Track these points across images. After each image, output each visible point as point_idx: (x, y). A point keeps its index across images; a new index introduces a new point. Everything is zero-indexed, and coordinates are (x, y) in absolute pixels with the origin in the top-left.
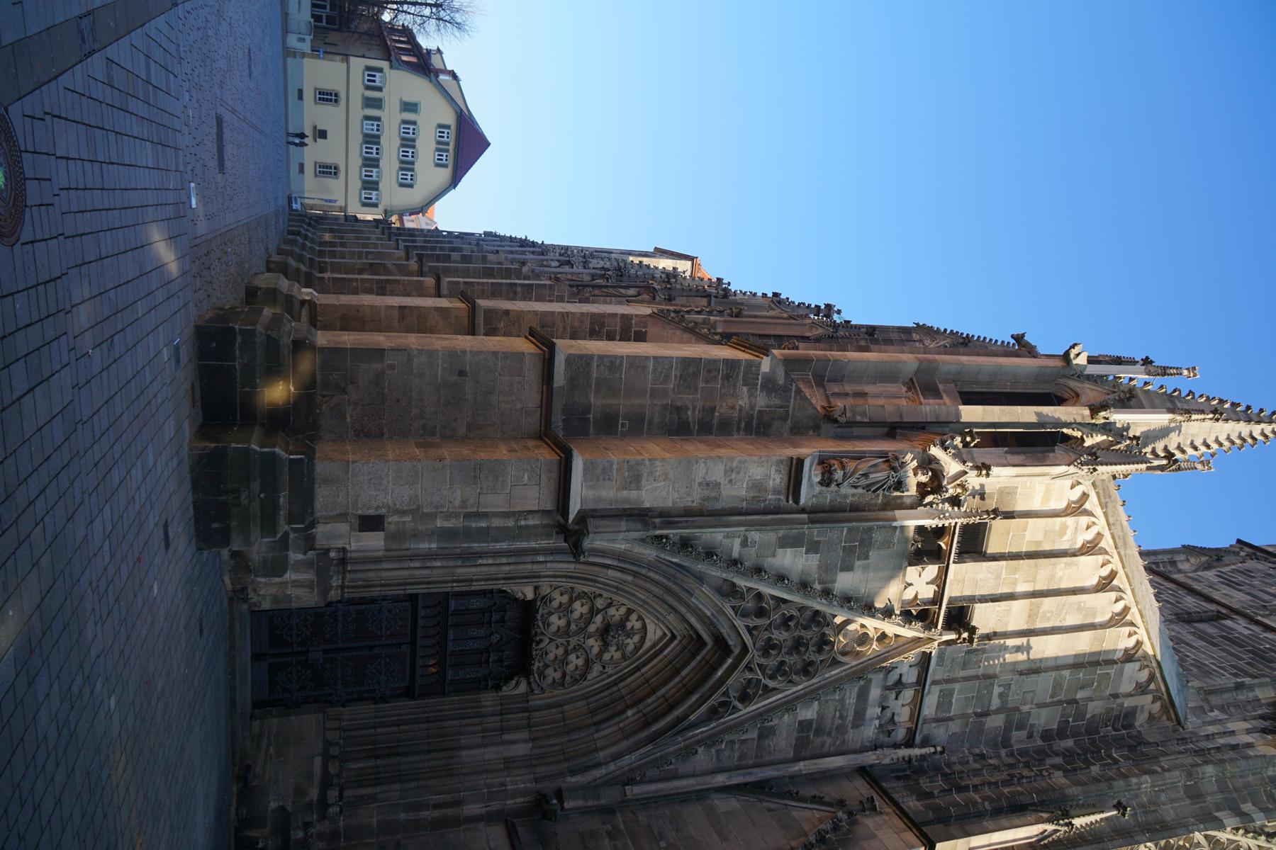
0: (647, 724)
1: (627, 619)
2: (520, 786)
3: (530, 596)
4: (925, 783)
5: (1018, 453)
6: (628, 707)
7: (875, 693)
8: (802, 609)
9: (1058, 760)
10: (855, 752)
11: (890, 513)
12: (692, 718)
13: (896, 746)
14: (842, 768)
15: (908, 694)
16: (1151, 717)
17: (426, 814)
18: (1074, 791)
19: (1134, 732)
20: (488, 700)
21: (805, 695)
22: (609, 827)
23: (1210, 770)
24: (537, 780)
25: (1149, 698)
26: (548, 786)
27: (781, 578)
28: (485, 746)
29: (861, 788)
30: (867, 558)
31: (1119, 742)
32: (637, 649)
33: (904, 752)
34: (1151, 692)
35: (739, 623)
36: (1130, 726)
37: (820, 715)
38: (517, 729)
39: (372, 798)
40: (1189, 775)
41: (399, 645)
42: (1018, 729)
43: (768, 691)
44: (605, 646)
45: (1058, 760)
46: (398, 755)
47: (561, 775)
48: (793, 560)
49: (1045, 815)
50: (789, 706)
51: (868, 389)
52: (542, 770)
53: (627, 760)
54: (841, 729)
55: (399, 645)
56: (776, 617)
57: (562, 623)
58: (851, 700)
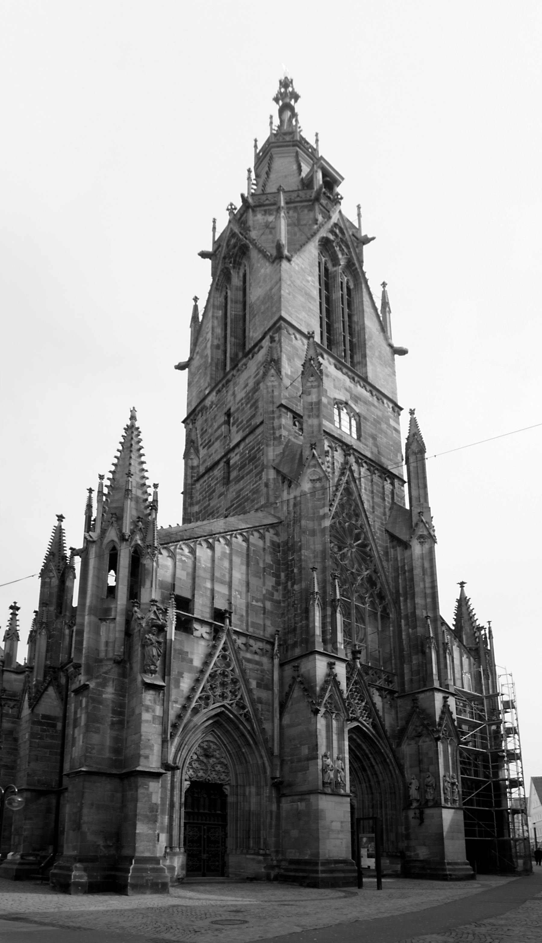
0: (249, 744)
1: (203, 747)
2: (267, 791)
3: (188, 783)
4: (290, 642)
5: (145, 582)
6: (241, 750)
7: (249, 656)
8: (208, 681)
9: (289, 583)
10: (273, 666)
11: (168, 641)
12: (249, 728)
13: (273, 649)
14: (279, 674)
15: (252, 642)
16: (277, 534)
17: (274, 823)
18: (304, 585)
19: (282, 544)
20: (231, 799)
21: (246, 685)
22: (289, 763)
23: (303, 522)
24: (266, 785)
25: (267, 533)
26: (269, 782)
27: (193, 690)
28: (250, 802)
29: (288, 670)
30: (187, 652)
31: (285, 553)
32: (216, 744)
33: (276, 648)
34: (264, 532)
35: (212, 707)
36: (279, 546)
37: (255, 679)
38: (244, 790)
39: (265, 839)
40: (304, 532)
41: (204, 829)
42: (273, 595)
43: (242, 698)
44: (213, 756)
45: (289, 583)
46: (249, 831)
47: (265, 777)
48: (186, 684)
49: (311, 602)
50: (250, 691)
51: (103, 639)
52: (263, 783)
53: (263, 754)
54: (262, 671)
55: (204, 829)
56: (210, 693)
57: (201, 772)
58: (250, 666)
